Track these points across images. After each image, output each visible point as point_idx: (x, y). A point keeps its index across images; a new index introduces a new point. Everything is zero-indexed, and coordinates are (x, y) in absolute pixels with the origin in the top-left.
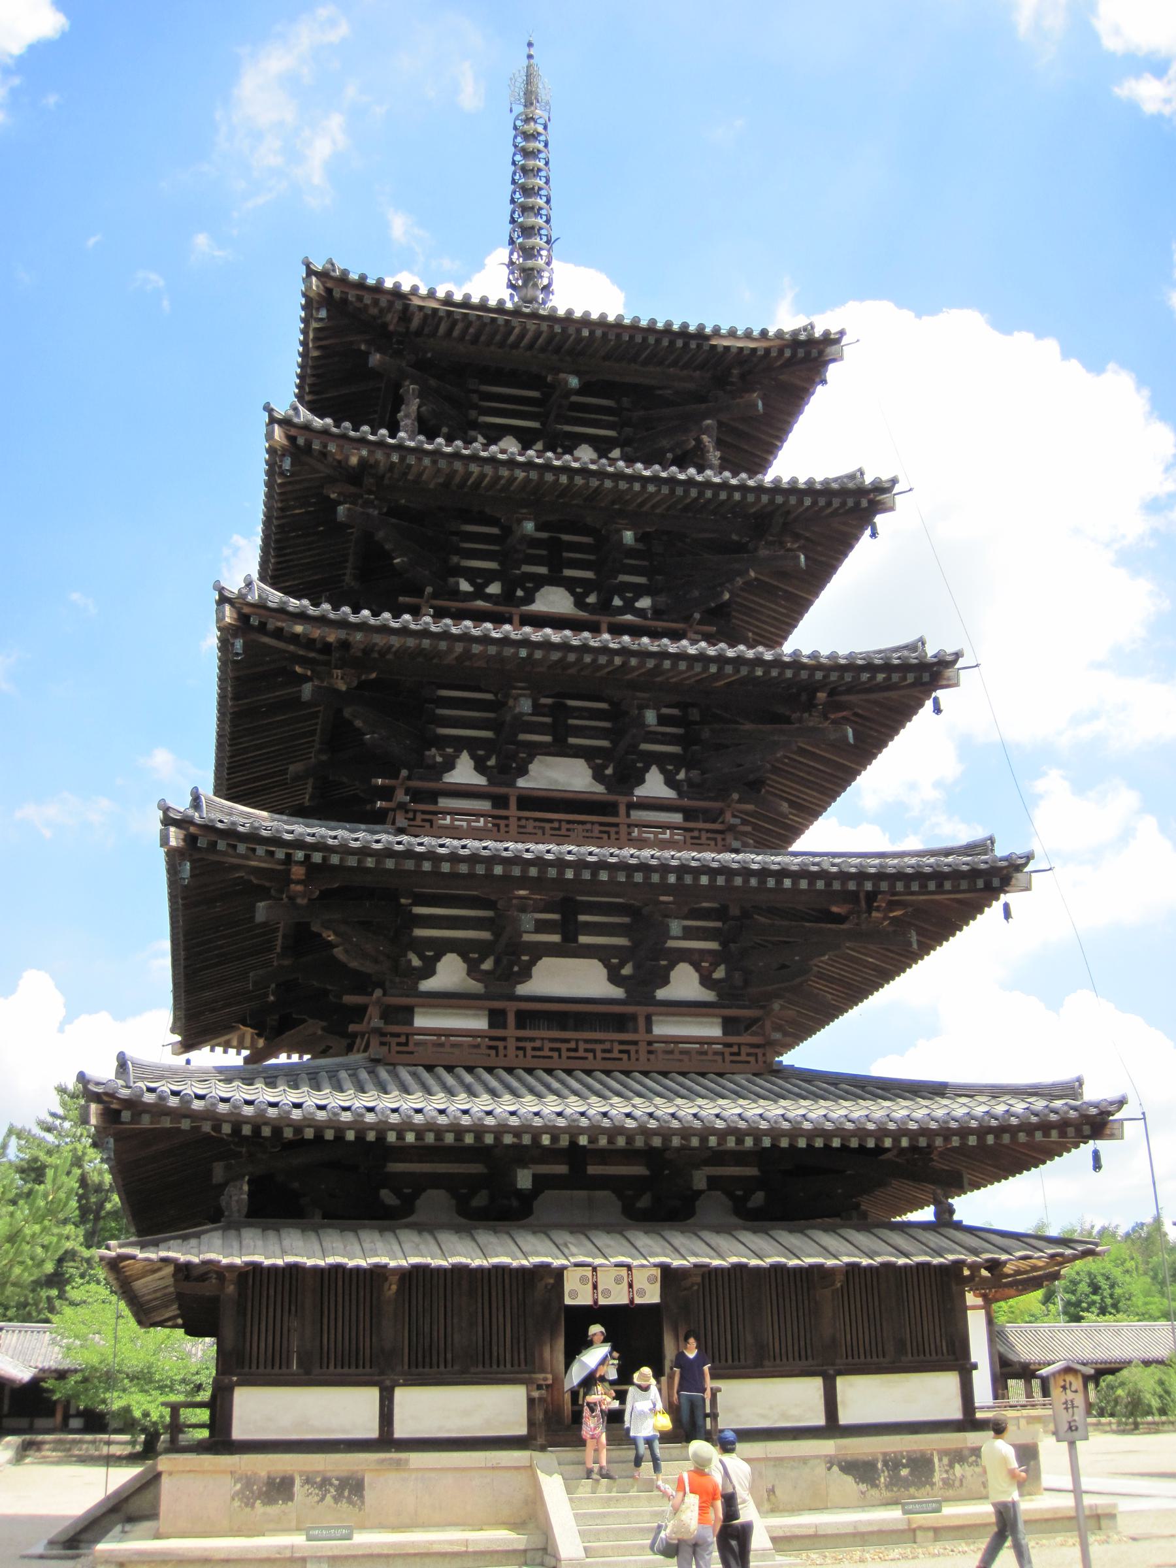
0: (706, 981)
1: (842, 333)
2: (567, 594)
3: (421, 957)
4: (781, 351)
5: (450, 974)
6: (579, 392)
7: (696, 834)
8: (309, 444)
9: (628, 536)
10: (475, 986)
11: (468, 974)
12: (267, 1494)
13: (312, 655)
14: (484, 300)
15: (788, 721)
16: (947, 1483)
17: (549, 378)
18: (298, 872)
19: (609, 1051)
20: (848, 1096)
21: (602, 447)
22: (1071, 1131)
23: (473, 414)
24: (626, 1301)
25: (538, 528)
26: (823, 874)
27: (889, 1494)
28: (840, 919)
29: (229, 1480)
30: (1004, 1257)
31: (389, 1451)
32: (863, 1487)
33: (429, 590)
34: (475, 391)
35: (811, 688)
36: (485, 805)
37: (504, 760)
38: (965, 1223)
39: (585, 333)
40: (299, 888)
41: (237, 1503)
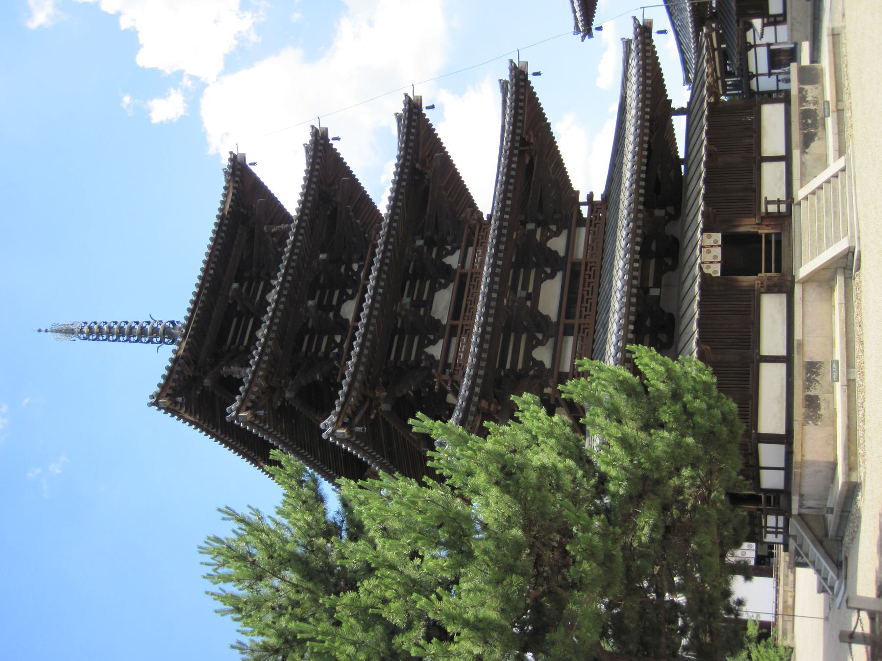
0: (557, 234)
1: (231, 153)
2: (346, 303)
3: (532, 368)
4: (236, 182)
5: (543, 354)
6: (241, 285)
7: (469, 302)
8: (252, 401)
9: (322, 256)
10: (551, 342)
11: (543, 345)
12: (814, 408)
13: (366, 405)
14: (189, 310)
15: (427, 188)
16: (815, 103)
17: (230, 301)
18: (484, 404)
19: (588, 292)
20: (623, 146)
21: (269, 288)
22: (648, 48)
23: (241, 348)
24: (720, 249)
25: (313, 299)
26: (511, 149)
28: (531, 161)
29: (807, 428)
30: (706, 84)
31: (793, 358)
32: (816, 139)
33: (336, 363)
34: (229, 347)
35: (414, 171)
36: (454, 340)
37: (432, 329)
38: (688, 100)
39: (211, 272)
40: (493, 406)
41: (819, 423)
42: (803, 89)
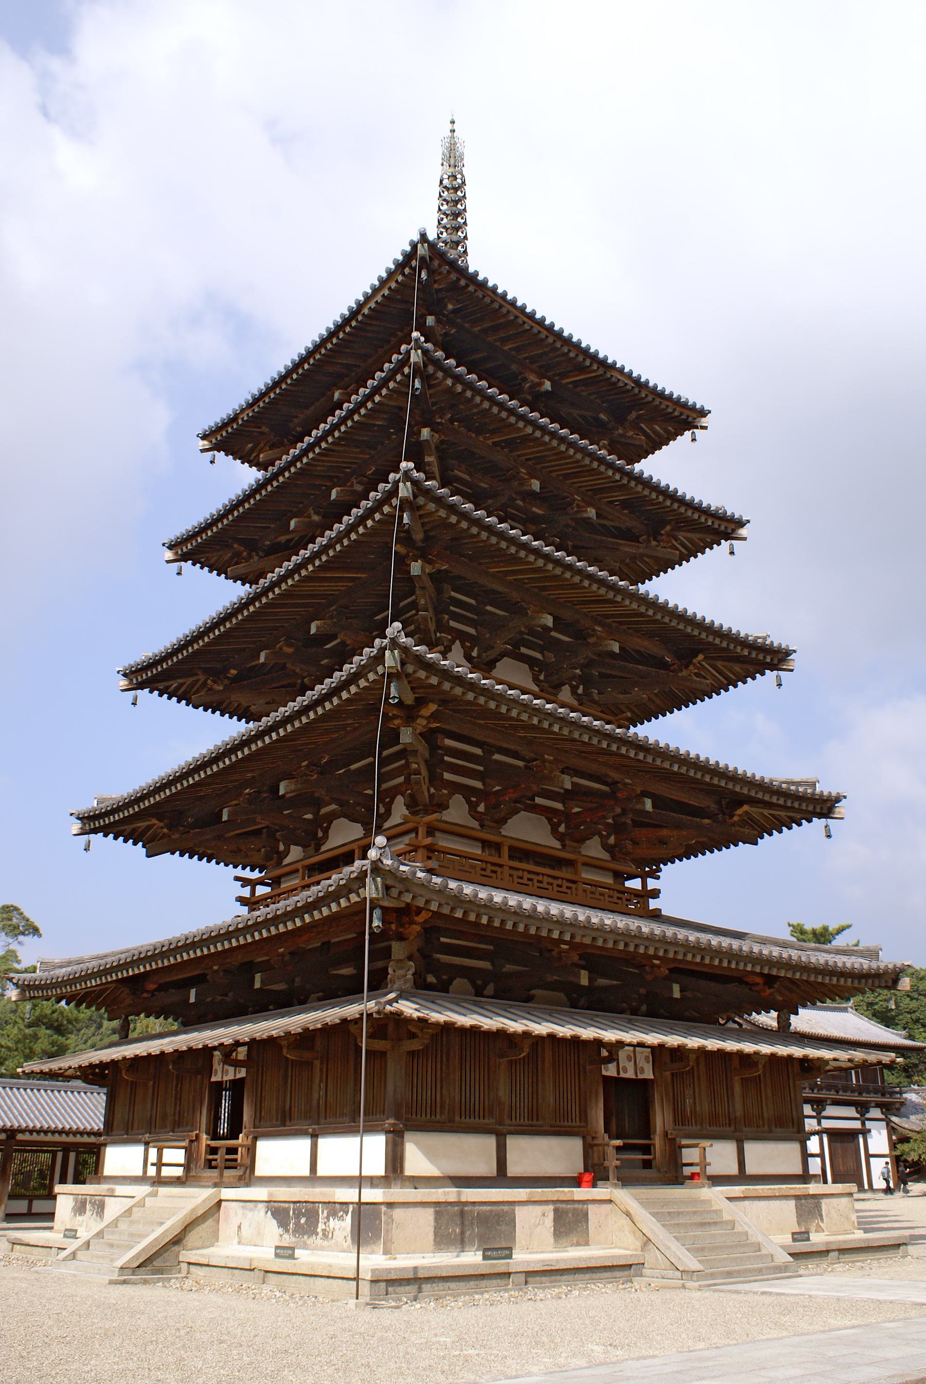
27: (294, 1239)
42: (347, 1213)
